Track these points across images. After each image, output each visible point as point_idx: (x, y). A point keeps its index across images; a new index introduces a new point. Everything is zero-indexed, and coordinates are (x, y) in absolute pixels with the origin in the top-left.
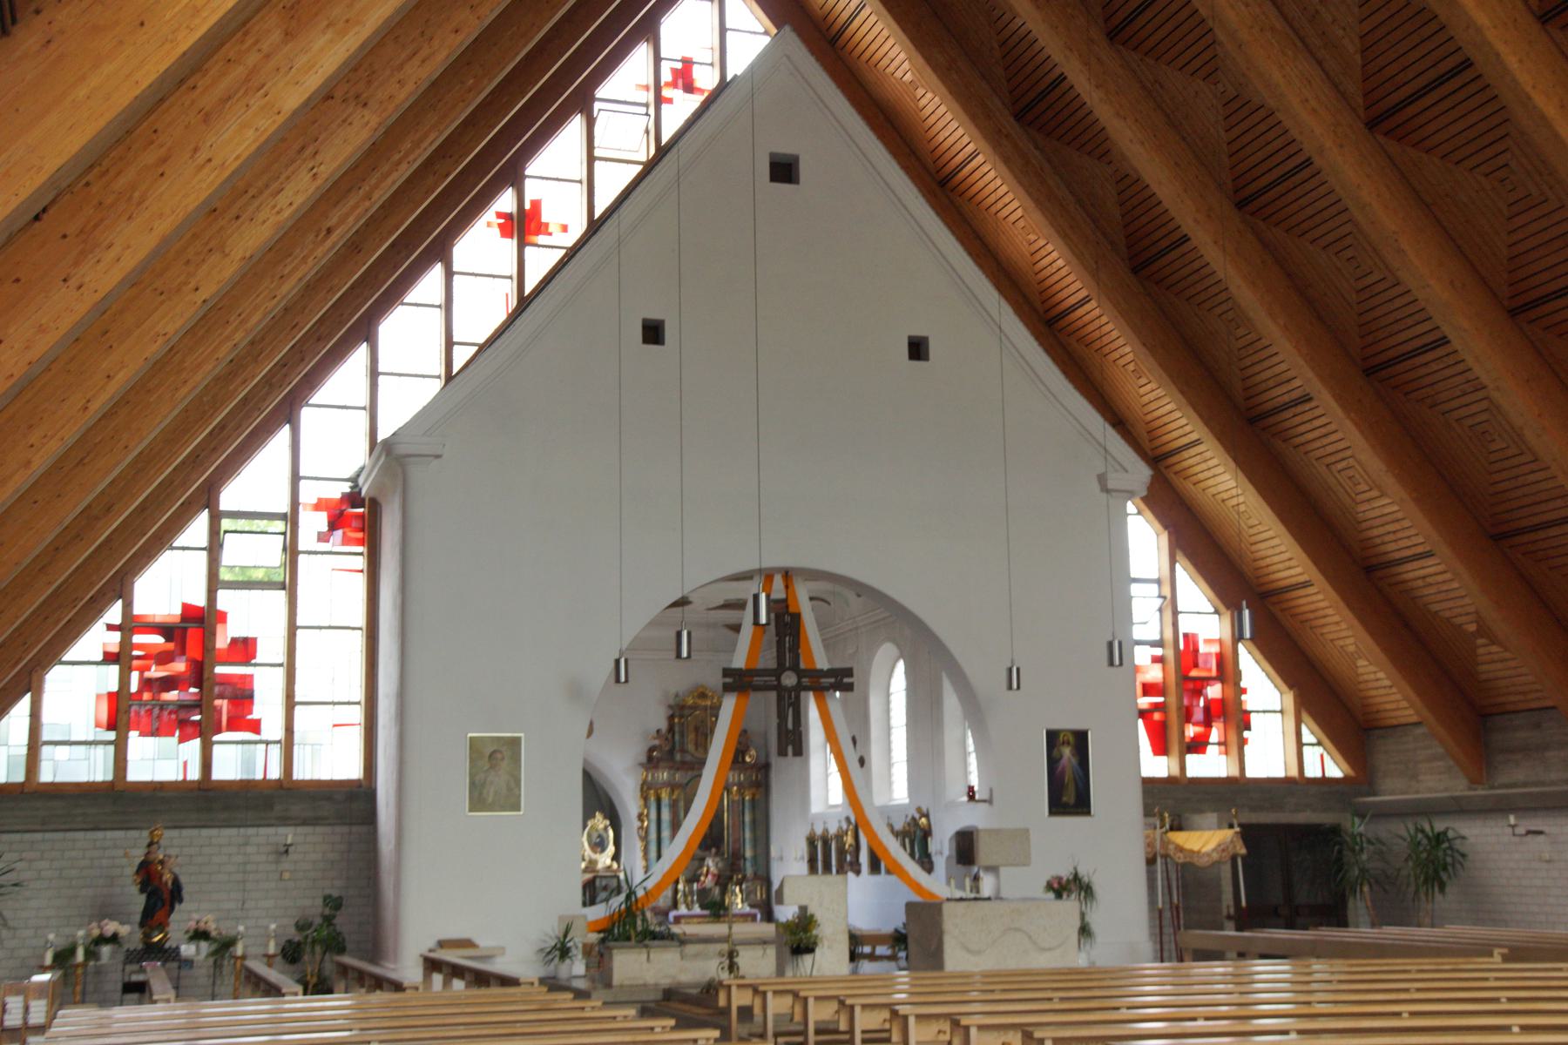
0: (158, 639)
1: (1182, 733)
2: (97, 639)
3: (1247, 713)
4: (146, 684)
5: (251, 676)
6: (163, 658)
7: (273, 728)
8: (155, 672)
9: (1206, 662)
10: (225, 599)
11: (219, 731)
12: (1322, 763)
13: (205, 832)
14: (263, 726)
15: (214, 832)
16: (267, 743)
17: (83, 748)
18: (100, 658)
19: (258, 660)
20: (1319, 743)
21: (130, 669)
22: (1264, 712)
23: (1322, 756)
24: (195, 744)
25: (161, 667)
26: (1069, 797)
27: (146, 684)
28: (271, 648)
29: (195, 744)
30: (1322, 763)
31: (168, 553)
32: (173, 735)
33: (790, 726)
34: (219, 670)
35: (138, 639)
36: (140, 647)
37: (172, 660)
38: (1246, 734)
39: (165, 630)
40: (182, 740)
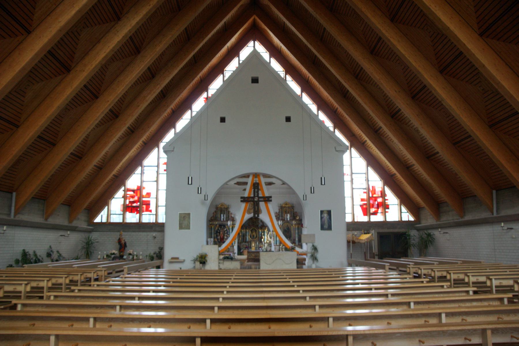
0: (132, 193)
1: (370, 211)
2: (120, 193)
3: (388, 205)
4: (130, 202)
5: (149, 201)
6: (133, 197)
7: (154, 212)
8: (132, 200)
9: (378, 193)
10: (144, 185)
11: (144, 212)
12: (407, 217)
13: (140, 233)
14: (152, 211)
15: (141, 233)
16: (153, 214)
17: (118, 215)
18: (122, 197)
19: (150, 197)
20: (408, 212)
21: (127, 199)
22: (393, 205)
23: (408, 215)
24: (138, 215)
26: (326, 226)
27: (130, 202)
28: (153, 195)
29: (138, 215)
30: (407, 217)
31: (134, 175)
32: (134, 212)
33: (256, 210)
34: (144, 199)
35: (128, 193)
36: (128, 195)
38: (387, 210)
39: (133, 191)
40: (137, 213)
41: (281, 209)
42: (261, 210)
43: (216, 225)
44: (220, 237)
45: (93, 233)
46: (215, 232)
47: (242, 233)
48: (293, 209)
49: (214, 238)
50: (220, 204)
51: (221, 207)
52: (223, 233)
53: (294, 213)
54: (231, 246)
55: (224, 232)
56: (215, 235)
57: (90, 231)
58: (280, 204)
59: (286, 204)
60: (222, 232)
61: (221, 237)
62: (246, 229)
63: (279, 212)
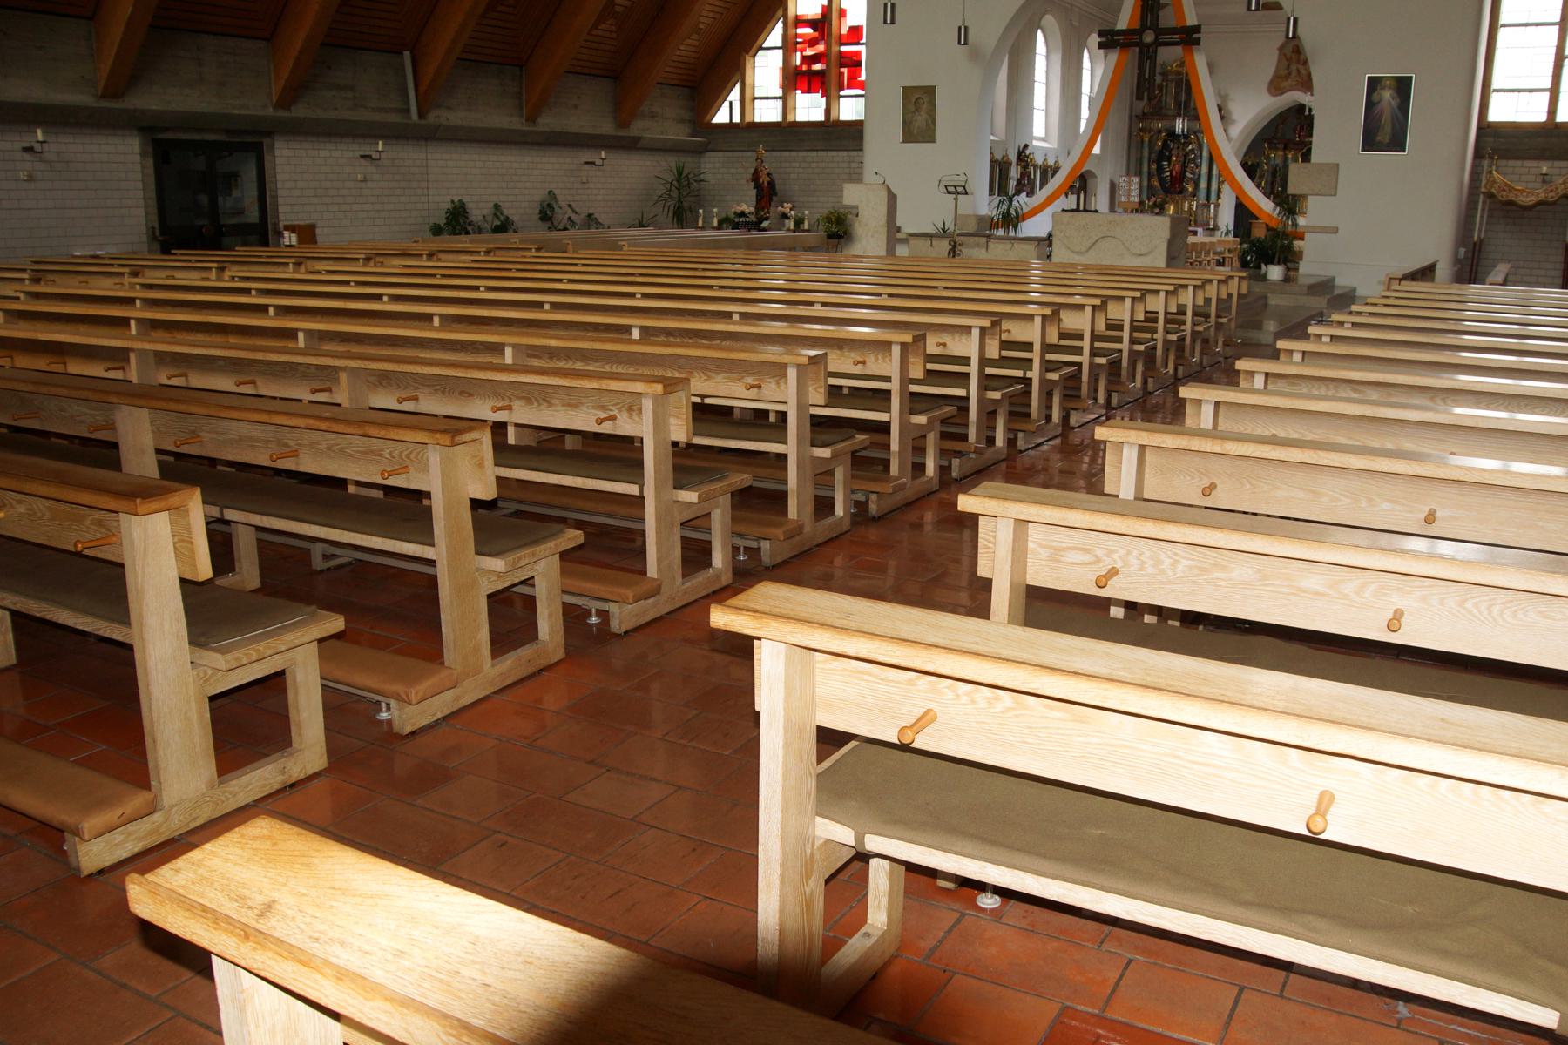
25: (811, 49)
37: (818, 44)
43: (1160, 132)
44: (1171, 171)
45: (708, 154)
46: (1154, 156)
47: (1272, 162)
49: (1150, 177)
50: (1175, 61)
51: (1180, 69)
52: (1182, 160)
54: (1204, 205)
55: (1186, 155)
56: (1154, 167)
57: (700, 151)
60: (1177, 157)
61: (1174, 173)
62: (1285, 148)
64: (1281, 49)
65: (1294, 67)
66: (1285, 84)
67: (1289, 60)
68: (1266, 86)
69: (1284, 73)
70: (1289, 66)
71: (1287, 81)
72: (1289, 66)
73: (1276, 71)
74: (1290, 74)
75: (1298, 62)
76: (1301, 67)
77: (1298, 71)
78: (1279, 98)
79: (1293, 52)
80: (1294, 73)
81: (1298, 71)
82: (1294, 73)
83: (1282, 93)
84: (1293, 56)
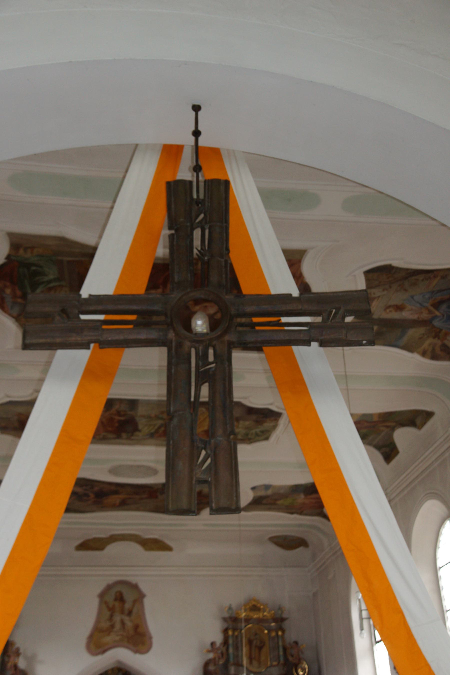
41: (234, 630)
42: (151, 638)
48: (283, 631)
53: (285, 649)
58: (230, 608)
59: (255, 608)
63: (225, 642)
64: (102, 596)
65: (117, 618)
66: (108, 639)
67: (112, 610)
68: (84, 641)
69: (105, 625)
70: (111, 616)
71: (109, 635)
72: (111, 616)
73: (98, 621)
74: (112, 626)
75: (122, 612)
76: (127, 620)
77: (123, 623)
78: (100, 657)
79: (116, 600)
80: (118, 626)
81: (123, 623)
82: (118, 626)
83: (104, 652)
84: (117, 604)
